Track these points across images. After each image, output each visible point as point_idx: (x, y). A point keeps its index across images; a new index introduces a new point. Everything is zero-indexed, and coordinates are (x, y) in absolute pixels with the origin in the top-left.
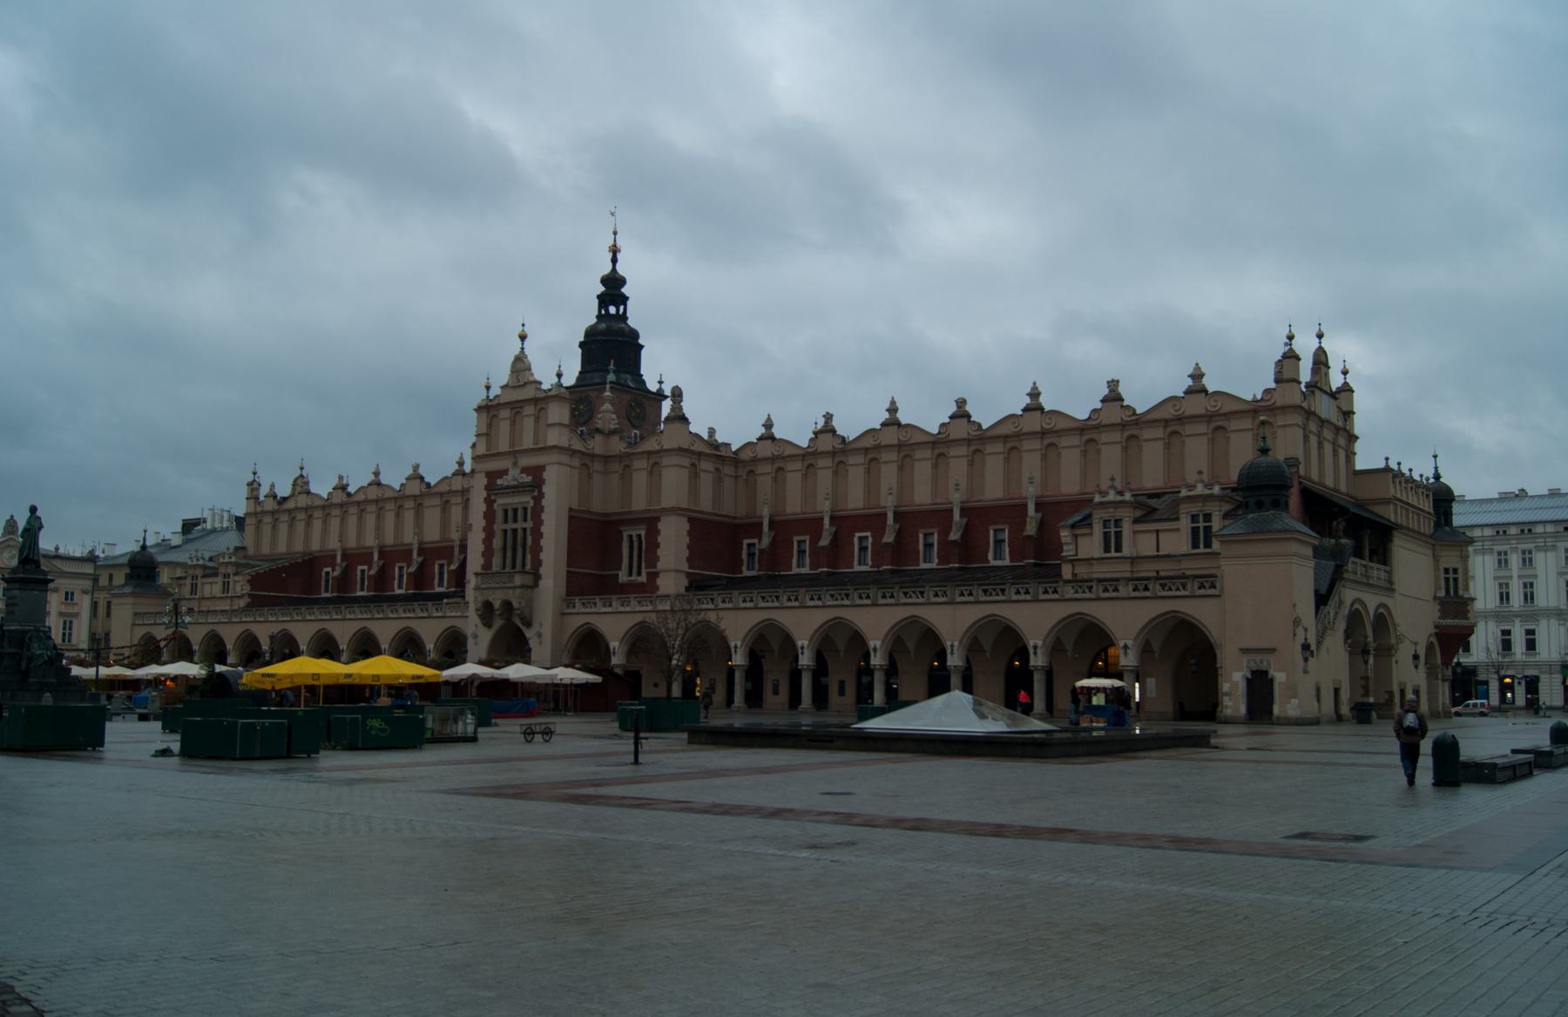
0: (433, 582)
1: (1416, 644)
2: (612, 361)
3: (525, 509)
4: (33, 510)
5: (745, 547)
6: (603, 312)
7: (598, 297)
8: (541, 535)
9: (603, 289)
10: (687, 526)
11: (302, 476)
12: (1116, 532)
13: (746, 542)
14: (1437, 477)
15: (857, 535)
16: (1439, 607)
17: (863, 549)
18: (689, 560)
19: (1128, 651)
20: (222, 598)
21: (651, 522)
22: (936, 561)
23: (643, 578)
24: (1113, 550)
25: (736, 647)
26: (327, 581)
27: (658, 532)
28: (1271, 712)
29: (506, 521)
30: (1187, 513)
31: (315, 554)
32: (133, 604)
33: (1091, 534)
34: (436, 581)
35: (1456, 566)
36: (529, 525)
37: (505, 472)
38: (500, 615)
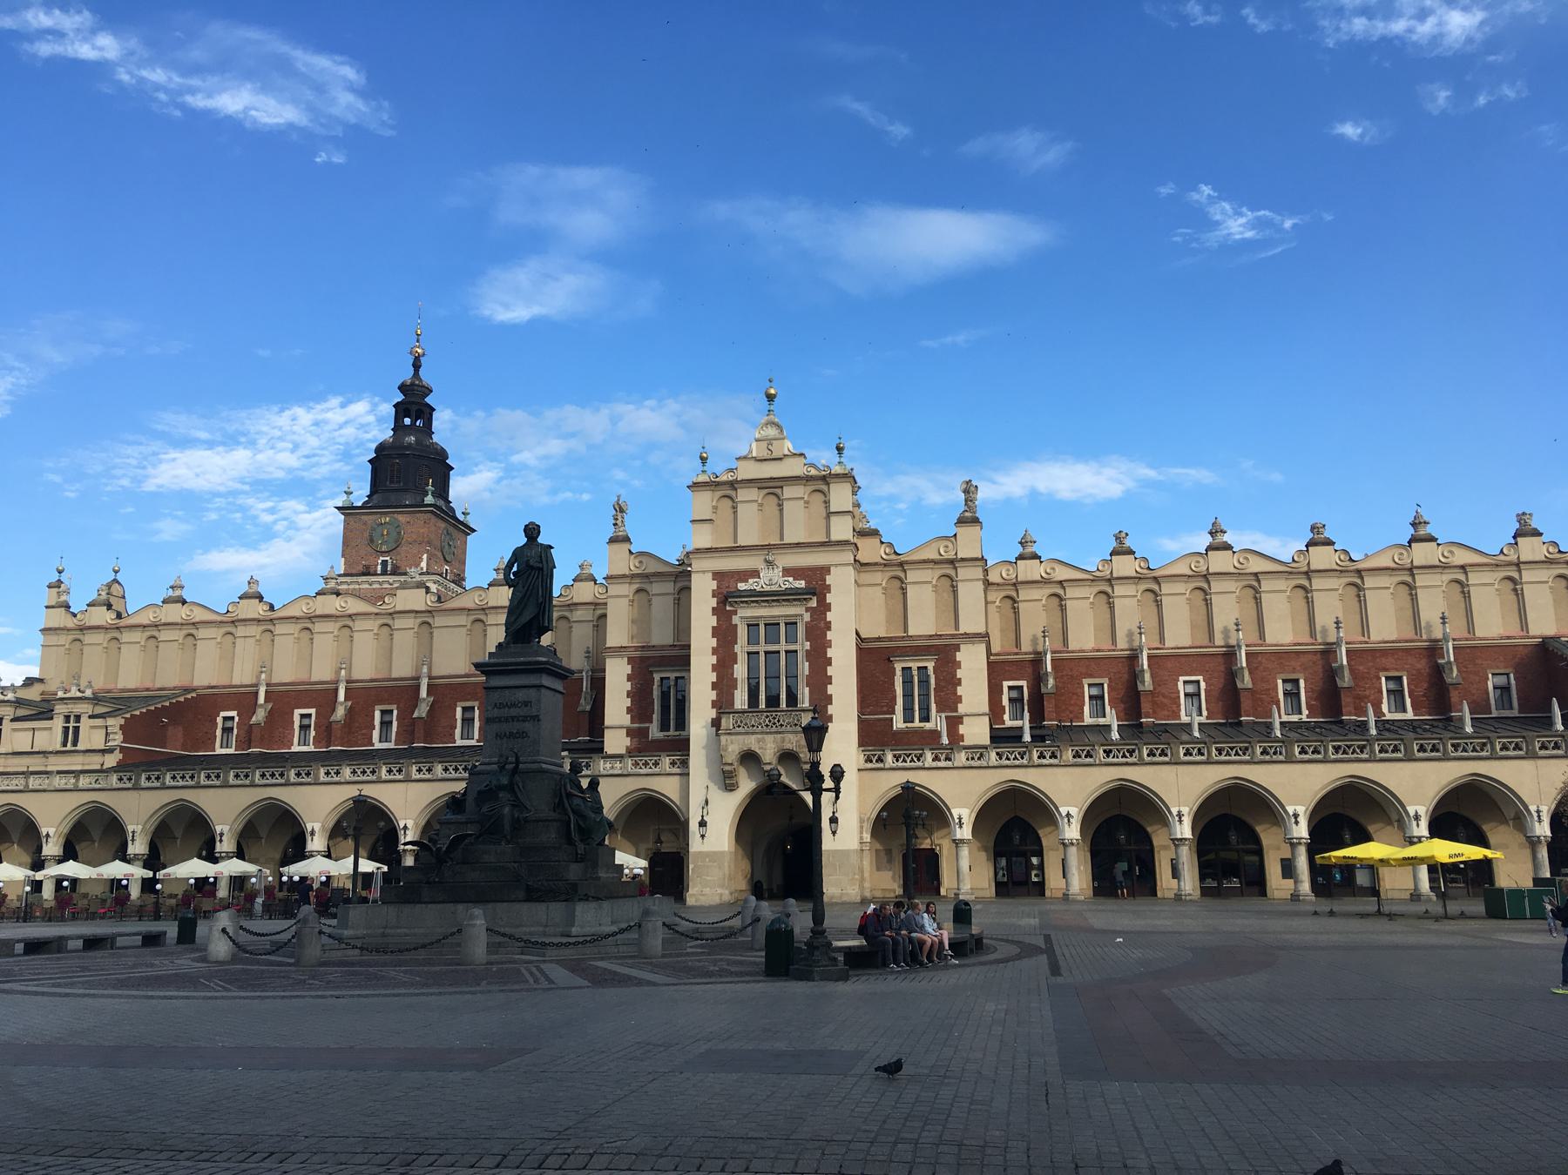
0: (452, 735)
2: (431, 481)
3: (791, 624)
4: (532, 531)
8: (829, 662)
9: (400, 397)
11: (116, 581)
15: (1182, 679)
20: (58, 752)
21: (944, 652)
22: (1305, 712)
25: (1180, 815)
27: (958, 665)
29: (754, 638)
34: (458, 732)
36: (802, 646)
37: (755, 573)
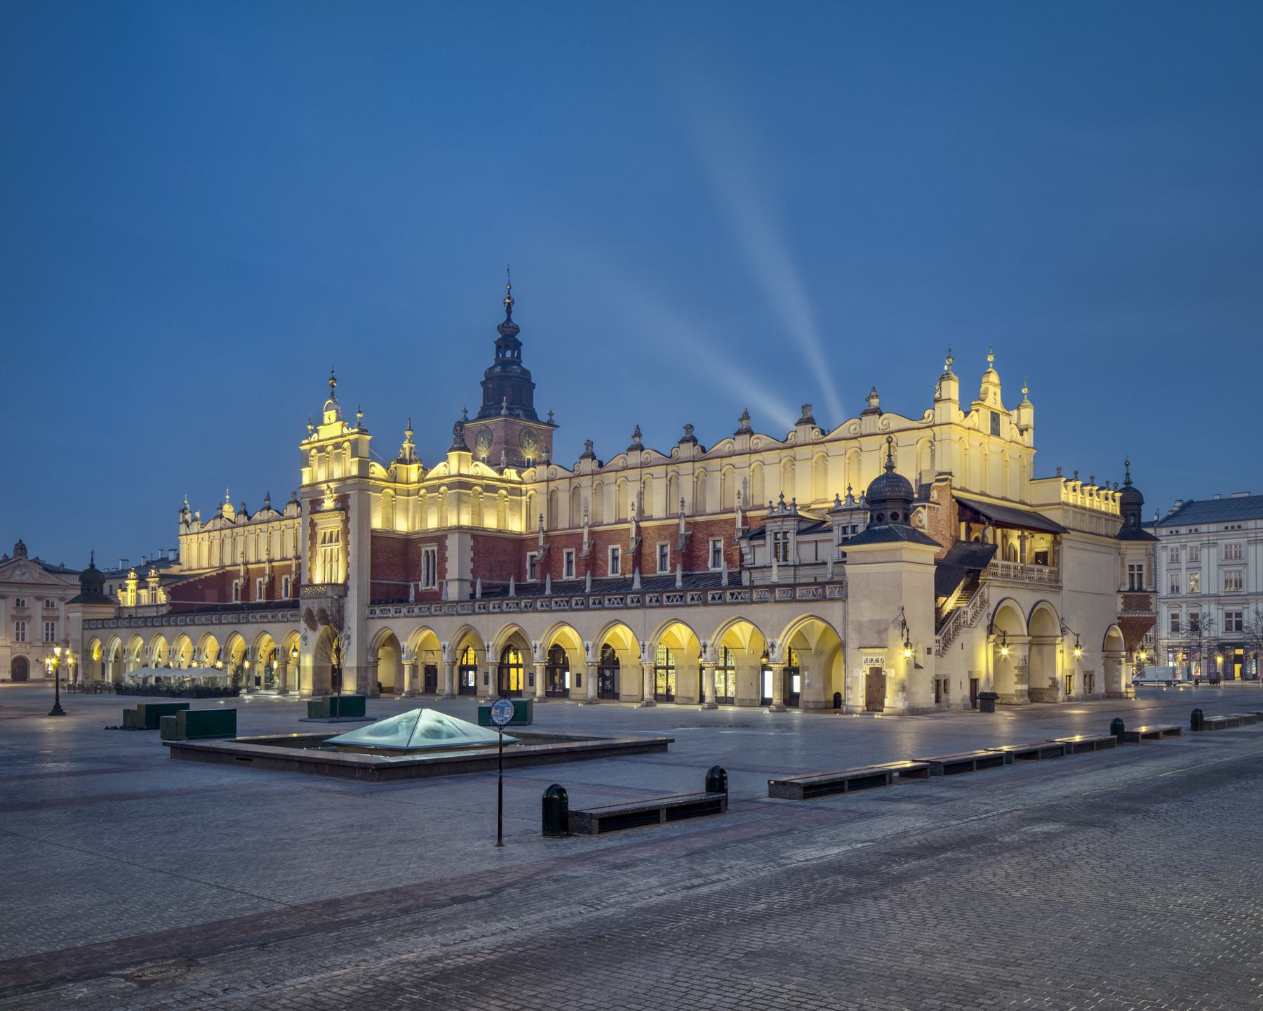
1: (1078, 635)
5: (528, 558)
6: (501, 356)
7: (495, 342)
10: (471, 543)
12: (784, 543)
13: (529, 554)
14: (1128, 483)
16: (1122, 600)
17: (615, 558)
18: (472, 571)
19: (775, 650)
22: (669, 568)
23: (436, 588)
24: (781, 560)
26: (237, 590)
28: (882, 704)
30: (839, 525)
31: (227, 568)
32: (82, 612)
33: (764, 545)
35: (1139, 563)
38: (320, 620)
